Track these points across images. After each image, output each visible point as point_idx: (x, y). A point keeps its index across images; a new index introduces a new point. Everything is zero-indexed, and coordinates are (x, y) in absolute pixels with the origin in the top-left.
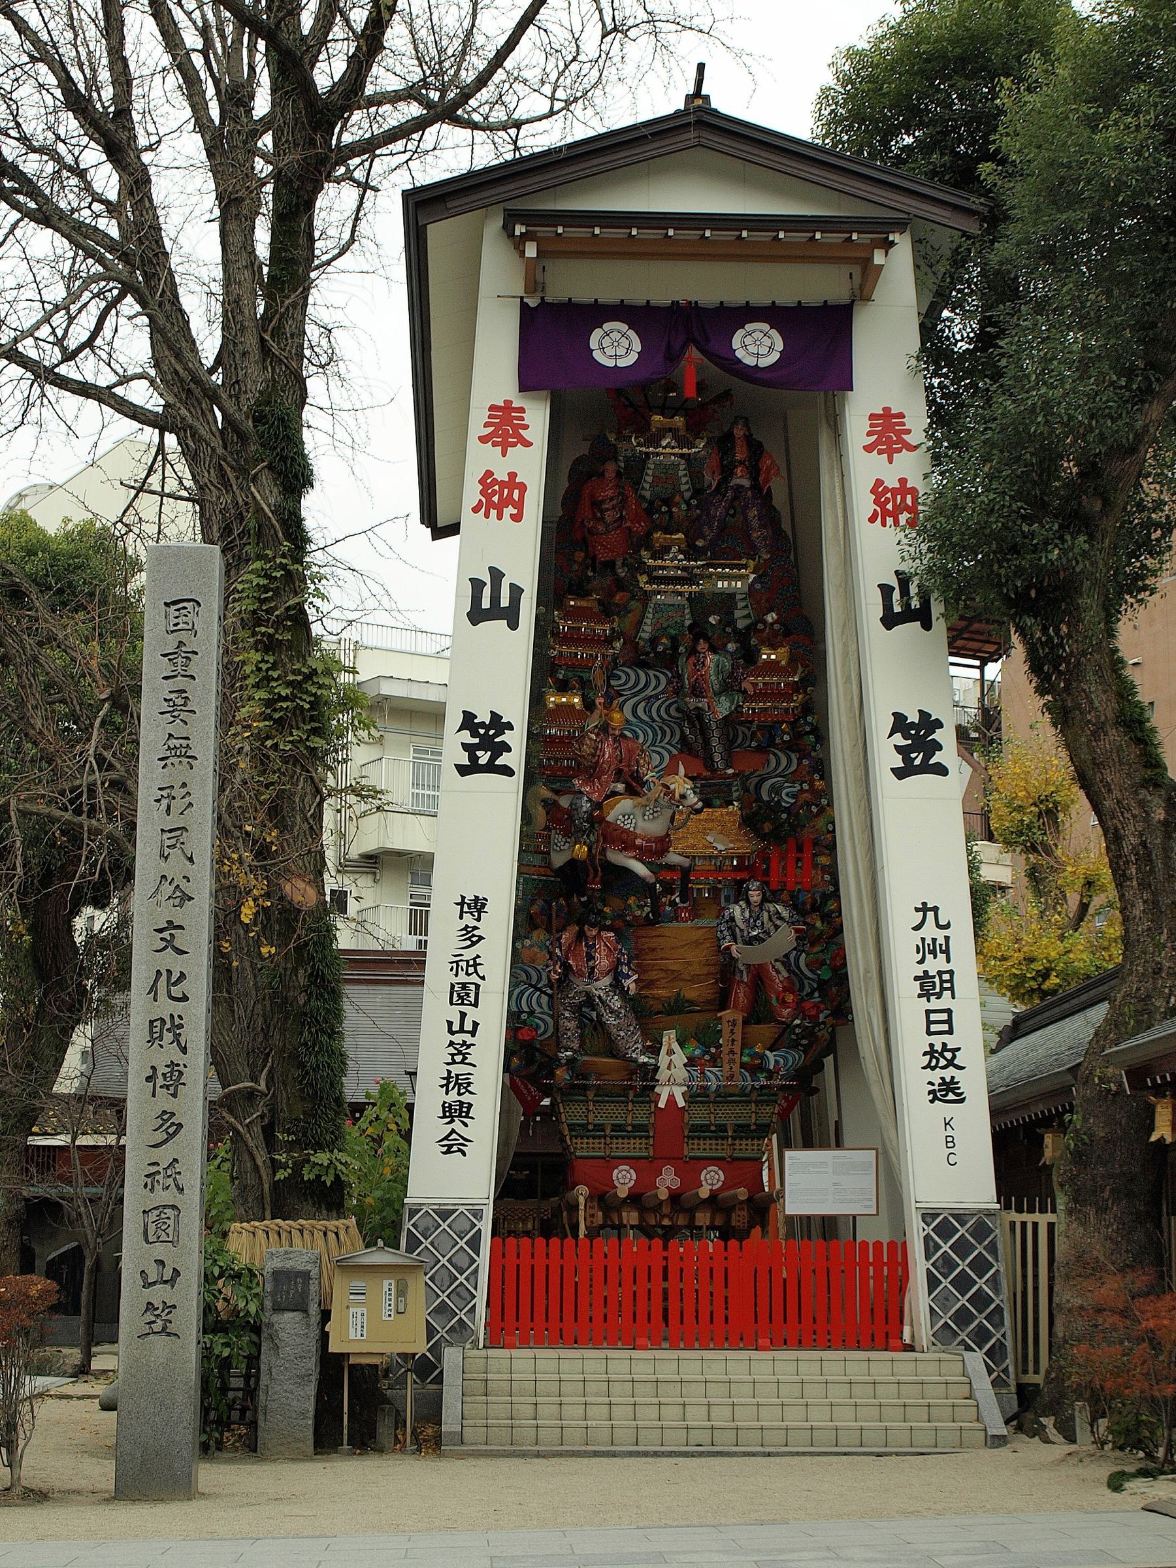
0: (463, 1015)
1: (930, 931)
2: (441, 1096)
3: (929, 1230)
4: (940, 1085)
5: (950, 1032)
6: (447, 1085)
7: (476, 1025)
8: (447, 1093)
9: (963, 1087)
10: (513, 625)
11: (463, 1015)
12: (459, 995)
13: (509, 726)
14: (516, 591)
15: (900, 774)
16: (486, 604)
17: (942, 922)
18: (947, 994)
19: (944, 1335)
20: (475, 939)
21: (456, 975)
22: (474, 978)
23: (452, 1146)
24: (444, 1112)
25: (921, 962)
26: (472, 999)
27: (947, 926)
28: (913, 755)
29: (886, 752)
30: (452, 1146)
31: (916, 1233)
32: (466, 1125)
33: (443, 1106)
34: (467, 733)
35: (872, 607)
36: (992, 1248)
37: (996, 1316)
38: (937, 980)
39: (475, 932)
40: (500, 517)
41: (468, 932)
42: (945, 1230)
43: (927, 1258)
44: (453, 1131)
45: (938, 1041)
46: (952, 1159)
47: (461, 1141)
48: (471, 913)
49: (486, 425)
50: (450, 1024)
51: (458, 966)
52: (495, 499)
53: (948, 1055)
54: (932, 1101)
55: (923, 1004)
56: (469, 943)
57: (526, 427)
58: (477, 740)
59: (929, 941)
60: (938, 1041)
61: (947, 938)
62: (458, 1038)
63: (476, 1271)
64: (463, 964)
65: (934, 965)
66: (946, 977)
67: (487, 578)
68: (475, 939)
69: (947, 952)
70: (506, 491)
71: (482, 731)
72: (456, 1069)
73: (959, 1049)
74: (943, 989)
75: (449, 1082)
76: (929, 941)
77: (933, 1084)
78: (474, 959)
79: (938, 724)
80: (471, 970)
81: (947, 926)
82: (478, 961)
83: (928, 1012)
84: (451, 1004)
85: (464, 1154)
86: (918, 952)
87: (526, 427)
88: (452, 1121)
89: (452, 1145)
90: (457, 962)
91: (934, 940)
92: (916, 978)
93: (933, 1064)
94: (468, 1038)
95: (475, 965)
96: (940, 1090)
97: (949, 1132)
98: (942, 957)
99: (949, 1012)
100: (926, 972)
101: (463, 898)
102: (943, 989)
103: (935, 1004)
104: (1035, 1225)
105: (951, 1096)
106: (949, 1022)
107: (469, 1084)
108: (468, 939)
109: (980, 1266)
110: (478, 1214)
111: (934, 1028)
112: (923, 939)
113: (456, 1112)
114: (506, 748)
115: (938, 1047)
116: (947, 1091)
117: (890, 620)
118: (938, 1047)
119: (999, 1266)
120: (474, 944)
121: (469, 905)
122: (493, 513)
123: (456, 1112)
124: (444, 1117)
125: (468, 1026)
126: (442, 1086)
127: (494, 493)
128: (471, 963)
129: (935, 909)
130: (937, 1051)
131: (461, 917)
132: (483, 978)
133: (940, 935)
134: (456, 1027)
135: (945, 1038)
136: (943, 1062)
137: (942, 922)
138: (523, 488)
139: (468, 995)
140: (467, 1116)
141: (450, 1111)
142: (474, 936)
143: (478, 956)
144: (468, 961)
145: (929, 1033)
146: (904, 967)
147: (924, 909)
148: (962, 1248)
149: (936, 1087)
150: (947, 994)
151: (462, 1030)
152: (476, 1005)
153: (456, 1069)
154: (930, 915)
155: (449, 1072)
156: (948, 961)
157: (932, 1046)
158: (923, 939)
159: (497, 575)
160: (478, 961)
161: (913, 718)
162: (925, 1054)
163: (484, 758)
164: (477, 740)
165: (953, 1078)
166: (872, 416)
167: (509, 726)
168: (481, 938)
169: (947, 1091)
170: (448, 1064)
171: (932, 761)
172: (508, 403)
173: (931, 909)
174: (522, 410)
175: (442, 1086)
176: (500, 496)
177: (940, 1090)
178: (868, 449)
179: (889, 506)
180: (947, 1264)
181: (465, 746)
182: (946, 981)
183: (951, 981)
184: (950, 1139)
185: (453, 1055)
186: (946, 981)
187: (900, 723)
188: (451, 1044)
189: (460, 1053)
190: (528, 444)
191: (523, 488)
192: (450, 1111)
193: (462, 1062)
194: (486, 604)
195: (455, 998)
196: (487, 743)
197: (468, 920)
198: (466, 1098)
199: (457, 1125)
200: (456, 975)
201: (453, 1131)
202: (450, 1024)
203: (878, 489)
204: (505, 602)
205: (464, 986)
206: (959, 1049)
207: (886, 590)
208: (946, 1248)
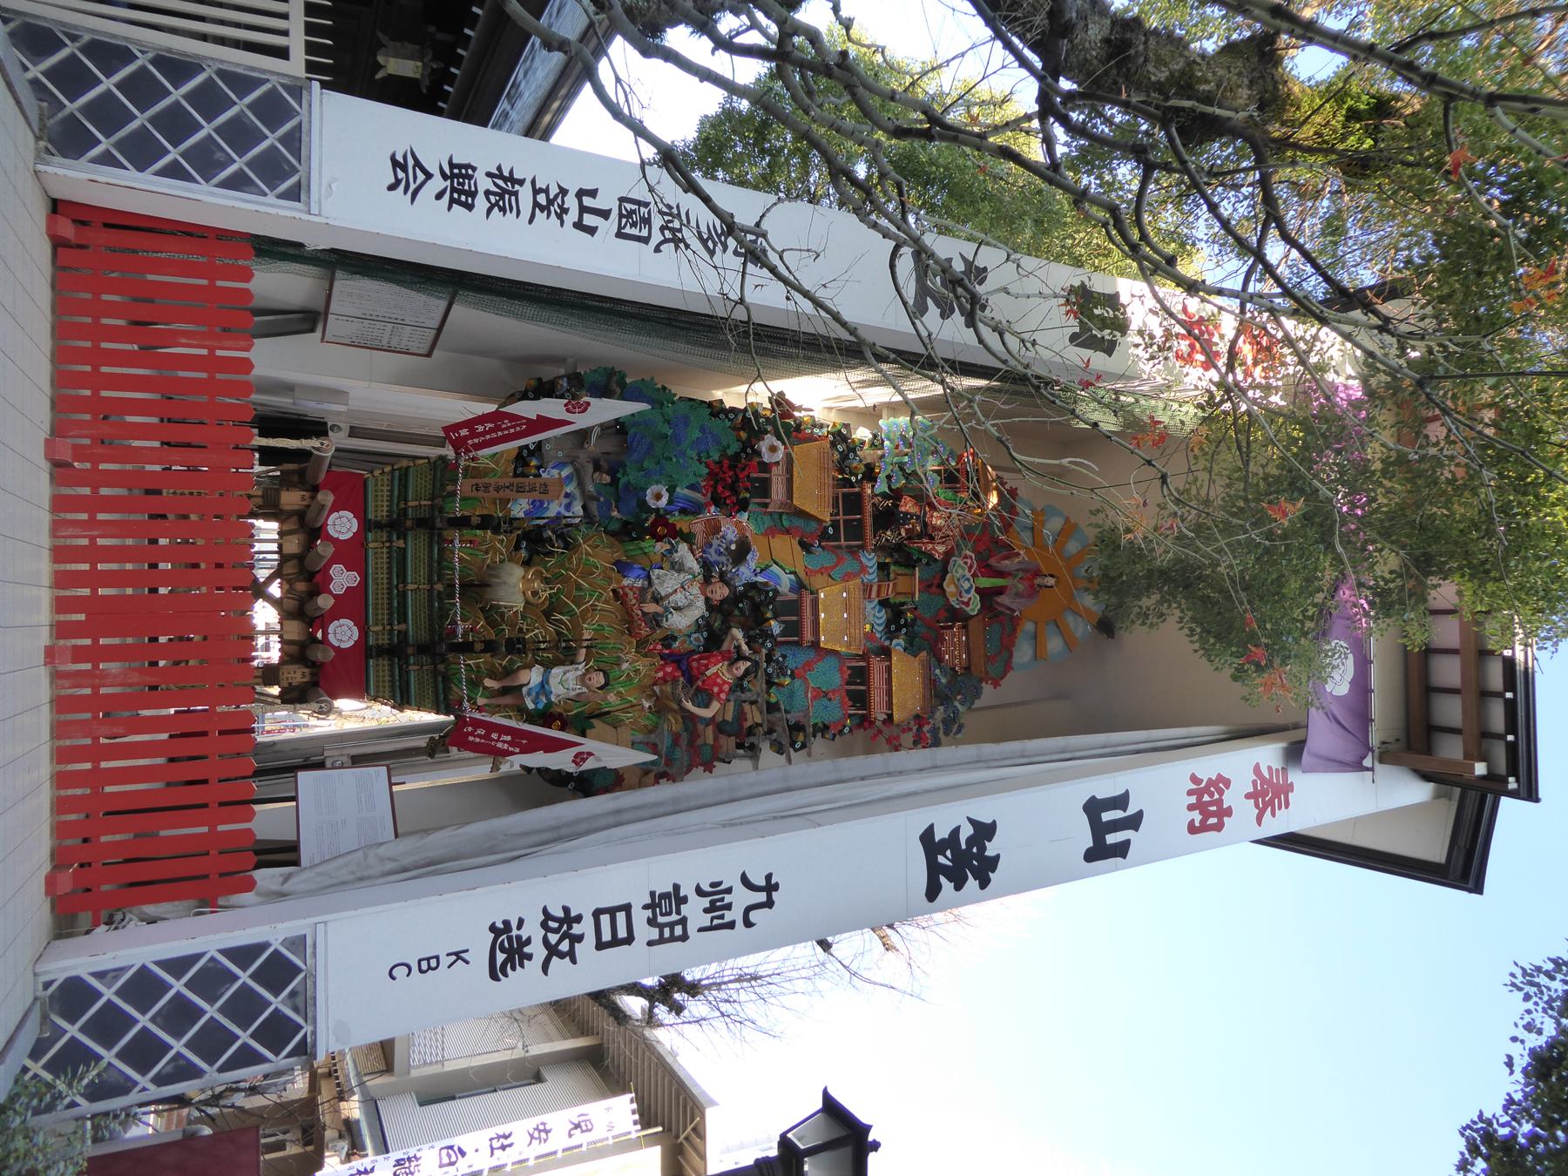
0: (605, 214)
1: (741, 898)
4: (519, 938)
5: (601, 945)
6: (501, 176)
7: (591, 231)
8: (489, 175)
9: (515, 976)
11: (605, 214)
12: (633, 212)
17: (753, 916)
18: (654, 934)
20: (710, 244)
22: (657, 237)
24: (460, 166)
25: (700, 892)
26: (628, 230)
27: (748, 924)
32: (439, 196)
33: (467, 166)
35: (1105, 787)
38: (674, 917)
39: (719, 248)
41: (719, 236)
44: (429, 176)
45: (586, 928)
46: (400, 972)
47: (413, 187)
55: (639, 900)
59: (728, 899)
60: (586, 928)
61: (731, 925)
62: (571, 202)
64: (676, 224)
65: (695, 911)
66: (678, 930)
68: (710, 244)
72: (525, 193)
73: (574, 961)
74: (661, 927)
76: (728, 899)
77: (519, 928)
78: (683, 240)
81: (748, 924)
83: (627, 908)
84: (622, 200)
85: (392, 188)
86: (713, 885)
90: (679, 215)
91: (728, 907)
92: (676, 887)
96: (510, 939)
97: (446, 961)
98: (706, 920)
100: (684, 900)
102: (661, 927)
103: (640, 917)
105: (500, 957)
106: (616, 942)
107: (503, 209)
108: (710, 237)
109: (212, 1043)
111: (605, 919)
112: (729, 891)
113: (459, 185)
115: (576, 929)
117: (1093, 808)
118: (576, 929)
120: (704, 242)
124: (452, 165)
125: (589, 220)
126: (499, 168)
129: (769, 904)
130: (570, 928)
132: (657, 250)
133: (735, 914)
134: (587, 201)
135: (590, 939)
136: (553, 938)
137: (753, 916)
139: (634, 225)
140: (452, 201)
141: (460, 176)
142: (715, 245)
144: (680, 230)
147: (770, 887)
148: (244, 1007)
149: (515, 932)
150: (654, 934)
151: (583, 209)
152: (620, 235)
153: (525, 193)
154: (762, 897)
155: (521, 182)
157: (579, 919)
158: (729, 891)
161: (991, 849)
162: (566, 910)
165: (529, 957)
170: (533, 182)
173: (769, 897)
177: (510, 939)
179: (1206, 798)
182: (672, 931)
183: (673, 939)
184: (433, 963)
186: (672, 931)
188: (563, 192)
189: (549, 203)
192: (460, 176)
193: (536, 204)
195: (629, 206)
198: (481, 203)
199: (438, 183)
201: (429, 176)
202: (593, 193)
203: (1221, 783)
205: (647, 221)
206: (574, 961)
207: (1121, 801)
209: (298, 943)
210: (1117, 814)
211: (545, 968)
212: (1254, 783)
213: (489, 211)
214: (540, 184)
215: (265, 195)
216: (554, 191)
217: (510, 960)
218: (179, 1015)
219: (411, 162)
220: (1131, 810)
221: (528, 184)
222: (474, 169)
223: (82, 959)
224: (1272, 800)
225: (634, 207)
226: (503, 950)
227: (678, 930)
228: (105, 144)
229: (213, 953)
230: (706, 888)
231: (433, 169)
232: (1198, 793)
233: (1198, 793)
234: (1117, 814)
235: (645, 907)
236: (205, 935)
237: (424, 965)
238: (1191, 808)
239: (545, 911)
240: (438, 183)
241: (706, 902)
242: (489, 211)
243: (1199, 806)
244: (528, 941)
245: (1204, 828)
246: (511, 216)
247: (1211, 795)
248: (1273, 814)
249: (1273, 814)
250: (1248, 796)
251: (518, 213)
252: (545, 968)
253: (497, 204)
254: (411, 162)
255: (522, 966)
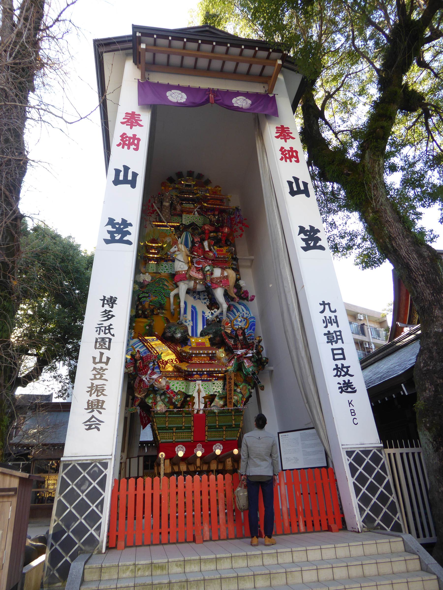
0: (102, 354)
1: (327, 313)
2: (87, 397)
3: (351, 460)
4: (343, 384)
5: (344, 359)
6: (90, 391)
7: (108, 359)
8: (90, 395)
9: (355, 385)
10: (133, 186)
11: (102, 354)
12: (100, 344)
13: (131, 225)
14: (135, 175)
15: (305, 249)
16: (121, 178)
17: (333, 309)
19: (368, 520)
20: (110, 316)
21: (99, 334)
22: (109, 335)
23: (91, 425)
24: (88, 406)
25: (326, 327)
26: (107, 346)
27: (335, 311)
28: (310, 242)
29: (298, 241)
30: (91, 425)
31: (345, 462)
32: (100, 413)
33: (88, 403)
34: (110, 226)
36: (383, 468)
37: (392, 508)
38: (334, 335)
39: (110, 313)
40: (129, 148)
41: (106, 313)
42: (359, 459)
43: (353, 476)
44: (93, 417)
45: (339, 363)
46: (356, 421)
47: (97, 422)
48: (108, 304)
49: (124, 119)
50: (94, 358)
51: (100, 329)
52: (127, 142)
53: (345, 370)
54: (341, 392)
56: (106, 318)
57: (141, 120)
58: (115, 230)
59: (328, 318)
60: (339, 363)
61: (336, 317)
62: (98, 366)
63: (102, 503)
64: (103, 329)
65: (332, 328)
66: (338, 333)
67: (122, 169)
68: (110, 316)
69: (337, 322)
70: (132, 140)
71: (117, 226)
72: (96, 382)
73: (349, 367)
75: (92, 390)
77: (340, 384)
78: (109, 326)
79: (318, 231)
80: (107, 331)
81: (335, 311)
82: (111, 327)
83: (333, 350)
85: (98, 429)
86: (324, 323)
87: (141, 120)
88: (93, 411)
89: (92, 425)
90: (100, 328)
91: (330, 317)
92: (325, 334)
93: (339, 374)
94: (104, 366)
95: (109, 329)
97: (352, 407)
98: (335, 325)
99: (342, 349)
100: (329, 332)
101: (104, 297)
103: (335, 346)
104: (394, 454)
105: (349, 390)
106: (343, 354)
107: (103, 390)
108: (107, 316)
109: (380, 478)
110: (105, 465)
111: (336, 357)
112: (325, 317)
113: (95, 406)
114: (130, 234)
115: (340, 366)
116: (347, 387)
117: (293, 193)
118: (340, 366)
119: (389, 478)
120: (109, 319)
121: (108, 302)
122: (126, 147)
123: (95, 406)
125: (104, 359)
126: (88, 392)
127: (127, 140)
128: (107, 328)
129: (329, 304)
130: (339, 368)
131: (103, 306)
132: (113, 335)
133: (333, 315)
134: (97, 360)
135: (342, 362)
136: (343, 373)
137: (333, 309)
138: (139, 140)
139: (105, 344)
142: (109, 315)
143: (111, 325)
144: (105, 327)
145: (335, 359)
146: (319, 330)
147: (324, 304)
148: (369, 469)
149: (342, 385)
150: (340, 341)
151: (101, 362)
152: (109, 349)
153: (96, 382)
154: (327, 307)
155: (92, 384)
156: (338, 326)
157: (337, 365)
158: (325, 317)
159: (126, 169)
160: (111, 327)
162: (334, 369)
163: (118, 237)
164: (115, 230)
165: (349, 381)
166: (277, 128)
167: (131, 225)
168: (113, 316)
169: (347, 387)
170: (92, 380)
171: (318, 245)
172: (133, 113)
174: (139, 115)
175: (88, 392)
176: (129, 142)
177: (344, 387)
178: (277, 137)
180: (361, 479)
181: (109, 232)
182: (339, 336)
183: (341, 335)
184: (352, 411)
185: (95, 375)
186: (339, 336)
187: (302, 230)
188: (95, 369)
189: (99, 373)
190: (142, 126)
191: (139, 140)
193: (100, 379)
194: (121, 178)
195: (98, 345)
196: (119, 231)
197: (107, 307)
198: (101, 398)
200: (99, 334)
201: (93, 417)
202: (94, 358)
204: (130, 178)
205: (103, 339)
206: (349, 367)
207: (290, 183)
208: (361, 469)
209: (349, 454)
210: (294, 185)
211: (352, 376)
212: (281, 139)
213: (104, 395)
214: (93, 377)
215: (106, 475)
216: (94, 372)
217: (350, 387)
218: (372, 489)
219: (88, 423)
220: (293, 180)
221: (93, 382)
222: (89, 401)
223: (356, 518)
224: (287, 133)
225: (98, 344)
226: (347, 389)
227: (338, 333)
228: (92, 531)
229: (354, 480)
230: (325, 325)
231: (90, 415)
232: (286, 158)
233: (286, 158)
234: (294, 185)
235: (332, 344)
236: (347, 483)
237: (353, 414)
238: (291, 161)
239: (335, 376)
240: (95, 413)
241: (329, 325)
242: (104, 395)
243: (290, 158)
244: (344, 381)
245: (297, 157)
246: (105, 387)
247: (286, 154)
248: (291, 133)
249: (291, 133)
250: (286, 141)
251: (104, 385)
252: (352, 376)
253: (101, 392)
254: (88, 423)
255: (351, 383)
